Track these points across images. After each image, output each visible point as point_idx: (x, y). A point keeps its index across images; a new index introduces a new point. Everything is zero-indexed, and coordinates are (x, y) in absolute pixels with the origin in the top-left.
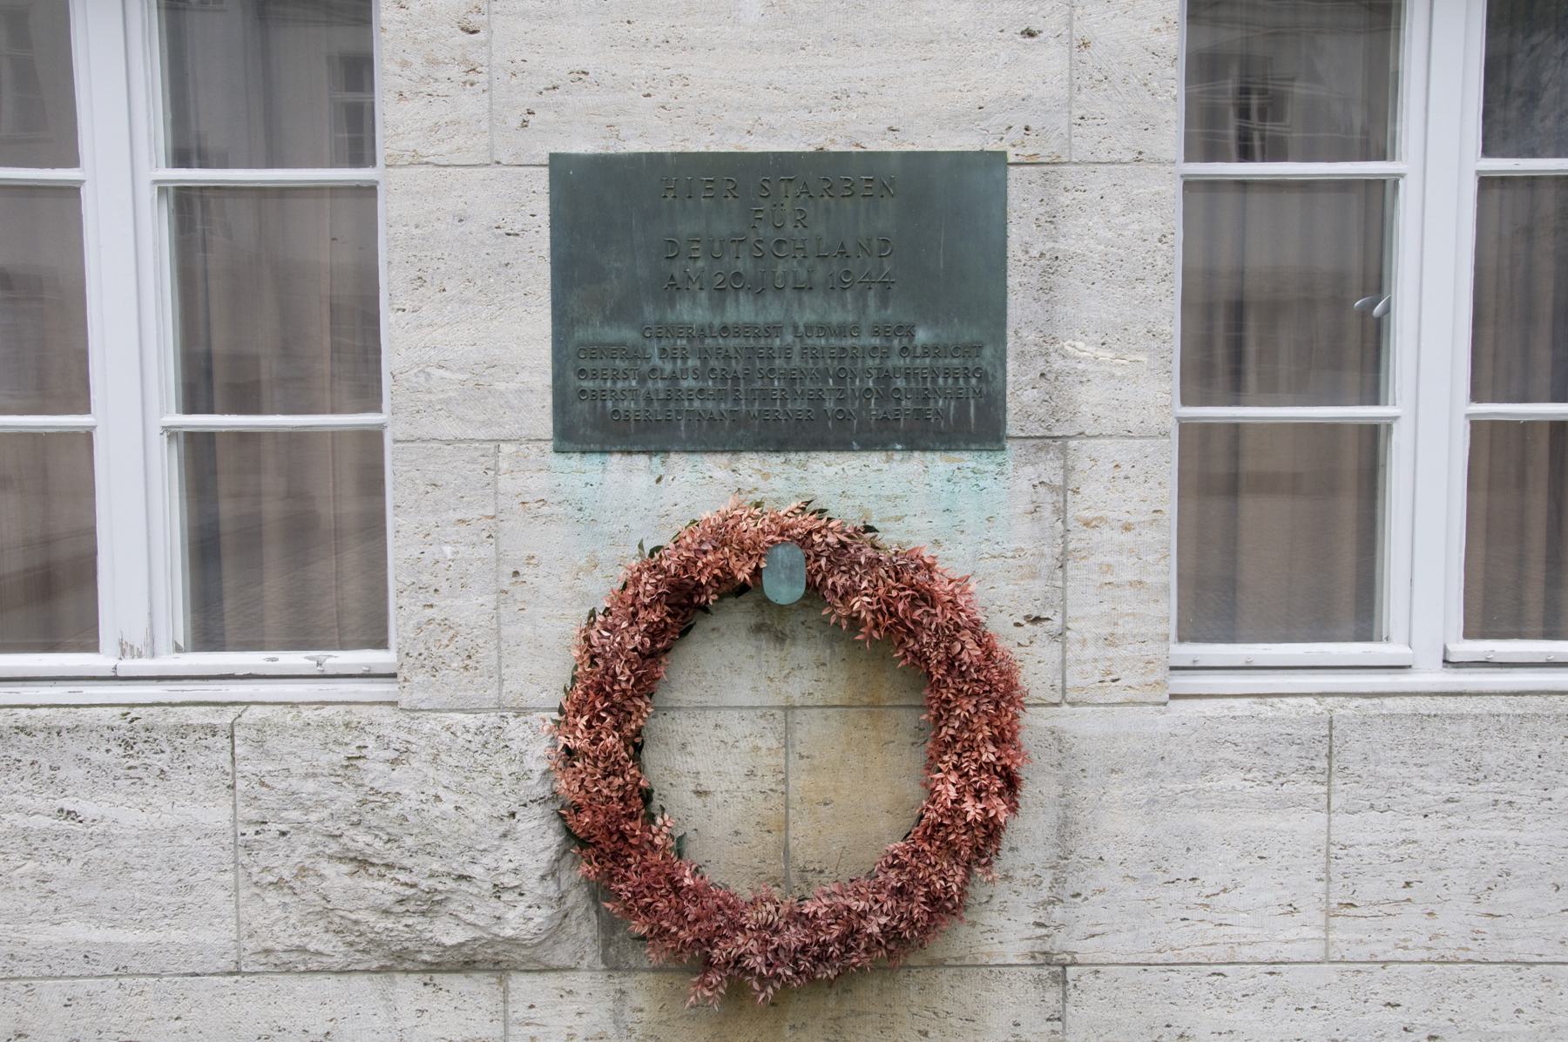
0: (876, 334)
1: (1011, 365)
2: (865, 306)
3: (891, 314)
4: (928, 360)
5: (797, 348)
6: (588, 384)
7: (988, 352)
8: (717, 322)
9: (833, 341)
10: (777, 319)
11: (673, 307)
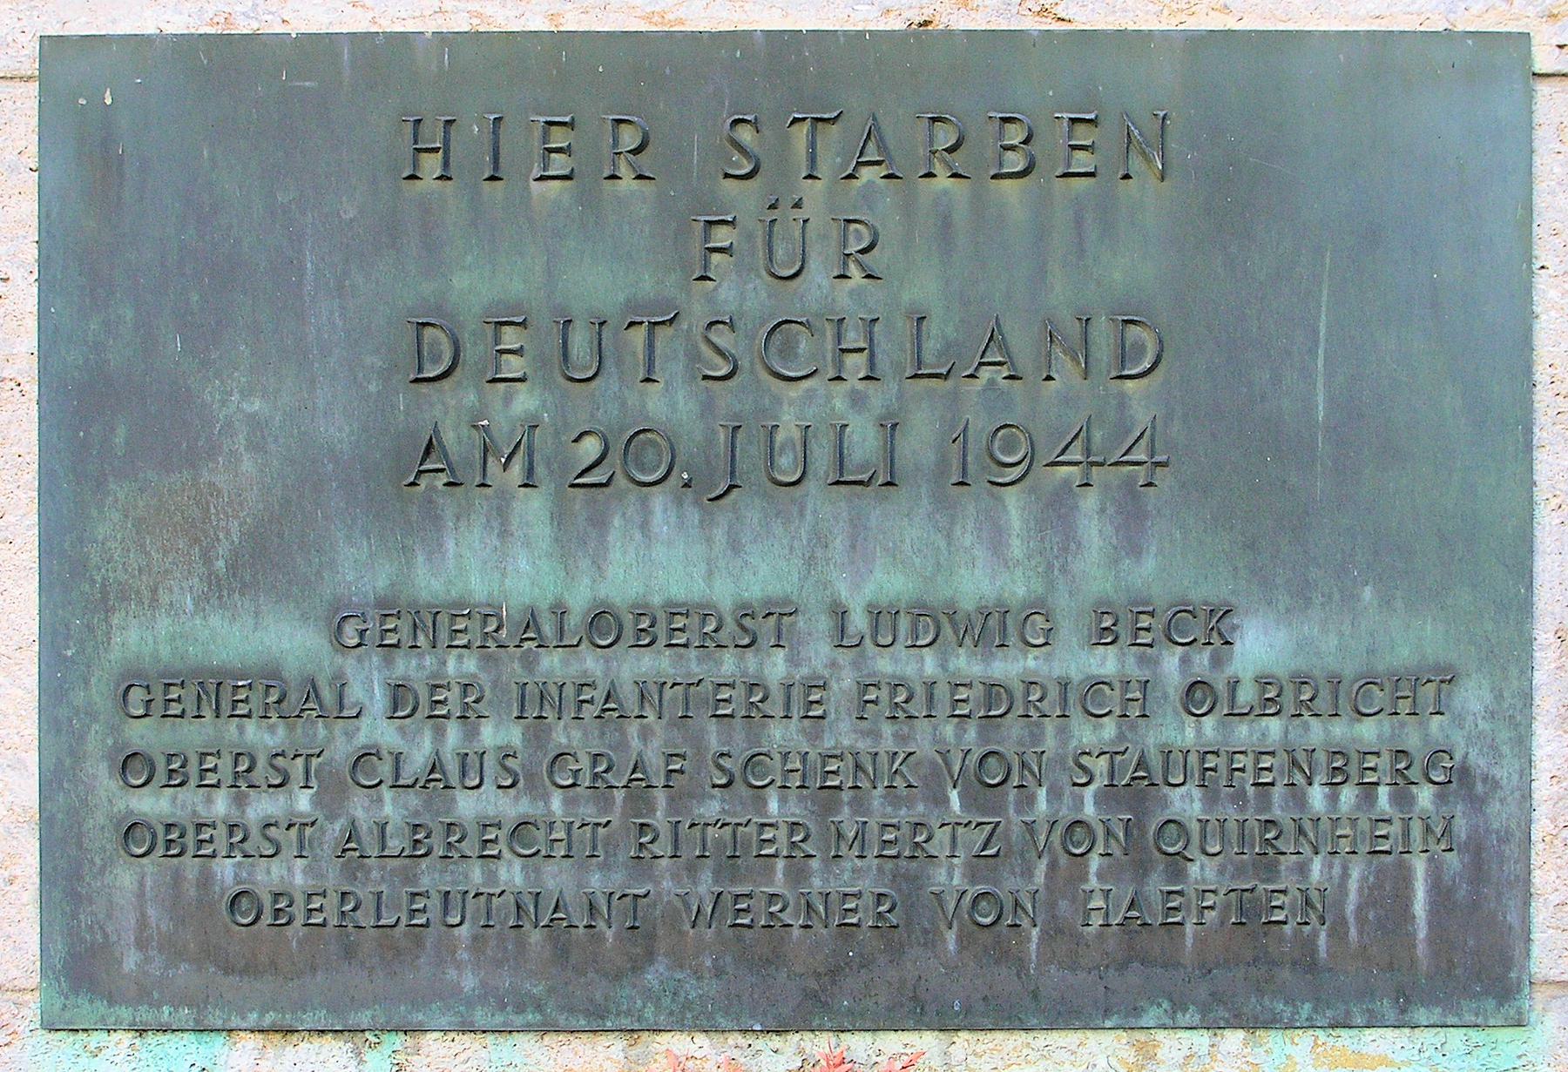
0: (1105, 636)
1: (1547, 745)
2: (1070, 541)
3: (1156, 573)
4: (1274, 726)
5: (846, 682)
6: (153, 804)
7: (1473, 696)
8: (579, 600)
9: (966, 663)
10: (776, 589)
11: (435, 549)
